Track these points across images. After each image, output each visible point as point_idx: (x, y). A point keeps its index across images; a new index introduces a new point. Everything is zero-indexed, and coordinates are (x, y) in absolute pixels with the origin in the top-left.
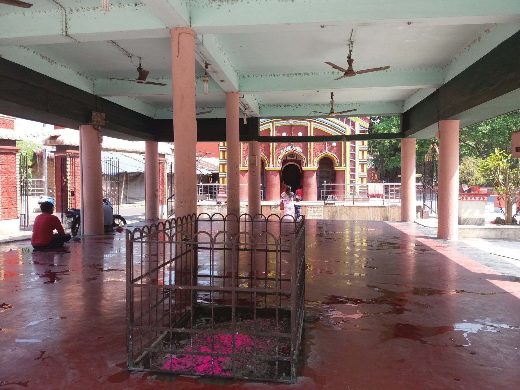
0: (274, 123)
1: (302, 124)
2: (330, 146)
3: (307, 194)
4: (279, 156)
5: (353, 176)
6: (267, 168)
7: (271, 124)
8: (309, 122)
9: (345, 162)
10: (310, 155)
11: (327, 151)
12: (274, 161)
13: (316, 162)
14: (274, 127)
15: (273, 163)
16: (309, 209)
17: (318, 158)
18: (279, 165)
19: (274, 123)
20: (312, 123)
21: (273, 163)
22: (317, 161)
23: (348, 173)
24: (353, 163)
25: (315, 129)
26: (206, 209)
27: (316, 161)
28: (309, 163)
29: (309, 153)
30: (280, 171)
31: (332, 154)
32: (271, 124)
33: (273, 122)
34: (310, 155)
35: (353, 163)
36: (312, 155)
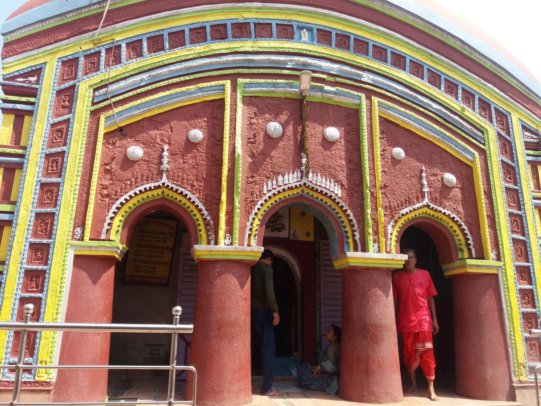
1: (337, 99)
3: (368, 372)
4: (254, 203)
6: (202, 249)
7: (228, 83)
8: (363, 96)
9: (497, 245)
10: (375, 209)
11: (426, 201)
12: (237, 220)
13: (394, 238)
14: (239, 96)
17: (399, 224)
18: (253, 242)
19: (240, 80)
20: (376, 100)
21: (230, 231)
22: (395, 233)
25: (384, 121)
27: (393, 233)
28: (371, 238)
29: (368, 201)
30: (255, 270)
31: (450, 213)
33: (233, 78)
34: (375, 209)
36: (381, 211)
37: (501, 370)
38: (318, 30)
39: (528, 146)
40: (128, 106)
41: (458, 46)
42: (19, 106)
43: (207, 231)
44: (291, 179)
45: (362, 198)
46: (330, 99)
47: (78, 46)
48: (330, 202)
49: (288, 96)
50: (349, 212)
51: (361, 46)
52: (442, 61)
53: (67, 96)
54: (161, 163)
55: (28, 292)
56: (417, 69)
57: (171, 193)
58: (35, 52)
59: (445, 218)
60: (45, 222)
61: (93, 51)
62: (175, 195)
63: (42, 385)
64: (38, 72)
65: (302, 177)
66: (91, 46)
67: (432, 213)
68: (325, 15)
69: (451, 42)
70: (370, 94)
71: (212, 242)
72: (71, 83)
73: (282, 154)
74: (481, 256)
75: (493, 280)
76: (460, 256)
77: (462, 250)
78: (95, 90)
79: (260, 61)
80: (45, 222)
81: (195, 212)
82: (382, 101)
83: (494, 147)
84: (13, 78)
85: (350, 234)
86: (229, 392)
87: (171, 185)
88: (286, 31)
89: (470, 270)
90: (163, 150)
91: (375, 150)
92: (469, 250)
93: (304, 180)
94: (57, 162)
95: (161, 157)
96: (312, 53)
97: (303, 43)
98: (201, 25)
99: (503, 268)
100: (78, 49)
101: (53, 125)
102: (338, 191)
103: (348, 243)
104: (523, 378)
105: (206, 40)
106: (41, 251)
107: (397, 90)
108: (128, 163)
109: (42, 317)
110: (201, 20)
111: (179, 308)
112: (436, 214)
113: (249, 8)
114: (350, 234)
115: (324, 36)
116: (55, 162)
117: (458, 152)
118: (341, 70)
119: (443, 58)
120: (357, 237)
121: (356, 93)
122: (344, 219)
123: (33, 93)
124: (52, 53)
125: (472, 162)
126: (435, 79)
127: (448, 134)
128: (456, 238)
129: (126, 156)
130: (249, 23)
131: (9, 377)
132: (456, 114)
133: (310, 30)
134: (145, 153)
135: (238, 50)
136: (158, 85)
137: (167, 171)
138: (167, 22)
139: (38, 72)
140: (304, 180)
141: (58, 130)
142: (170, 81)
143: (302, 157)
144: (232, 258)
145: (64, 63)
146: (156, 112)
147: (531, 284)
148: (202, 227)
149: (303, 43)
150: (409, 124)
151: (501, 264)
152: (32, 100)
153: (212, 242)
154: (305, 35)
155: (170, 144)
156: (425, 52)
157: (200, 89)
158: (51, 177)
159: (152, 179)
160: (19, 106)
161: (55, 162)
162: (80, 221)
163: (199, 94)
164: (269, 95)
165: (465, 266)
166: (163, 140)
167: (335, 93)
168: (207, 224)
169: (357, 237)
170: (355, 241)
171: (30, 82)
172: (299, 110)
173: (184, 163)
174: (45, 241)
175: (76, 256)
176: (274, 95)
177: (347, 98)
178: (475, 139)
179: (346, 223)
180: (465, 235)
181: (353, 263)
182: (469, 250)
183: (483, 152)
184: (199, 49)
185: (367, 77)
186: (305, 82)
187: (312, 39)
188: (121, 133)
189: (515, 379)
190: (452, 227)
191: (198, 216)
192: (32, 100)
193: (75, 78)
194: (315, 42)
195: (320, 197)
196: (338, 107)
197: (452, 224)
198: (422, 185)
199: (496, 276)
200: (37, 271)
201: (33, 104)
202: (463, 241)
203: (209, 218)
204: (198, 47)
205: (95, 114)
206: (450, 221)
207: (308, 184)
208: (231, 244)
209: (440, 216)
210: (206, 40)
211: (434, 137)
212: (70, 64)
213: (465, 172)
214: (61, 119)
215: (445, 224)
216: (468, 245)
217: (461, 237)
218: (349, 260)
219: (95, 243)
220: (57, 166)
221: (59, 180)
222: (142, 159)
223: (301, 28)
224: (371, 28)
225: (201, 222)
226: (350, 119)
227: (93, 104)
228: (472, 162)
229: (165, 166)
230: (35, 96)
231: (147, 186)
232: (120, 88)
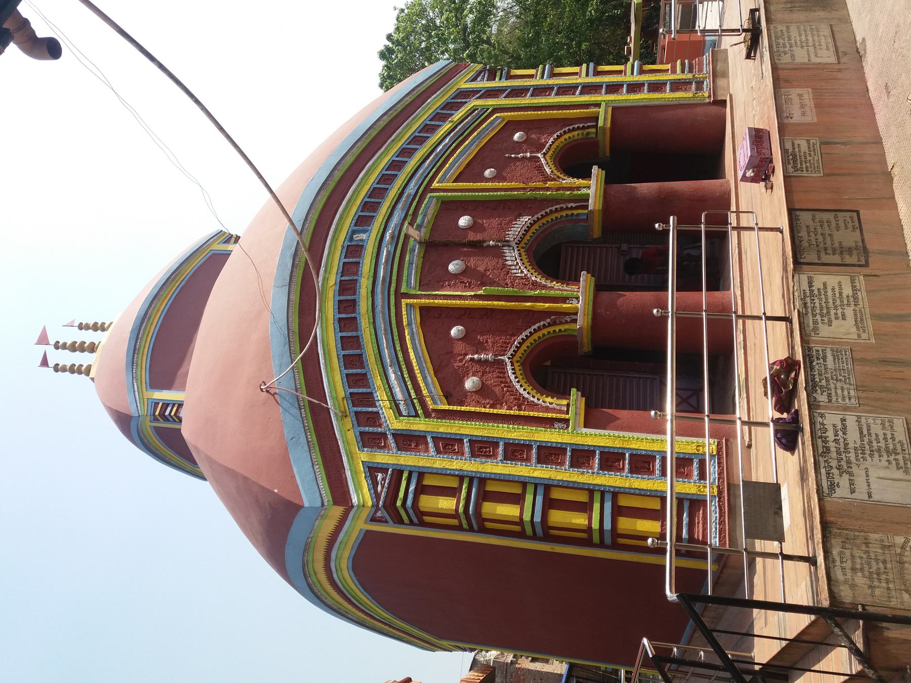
0: (403, 289)
2: (525, 147)
5: (634, 87)
7: (404, 302)
8: (429, 195)
11: (539, 155)
15: (564, 300)
16: (785, 59)
19: (403, 289)
20: (435, 185)
21: (564, 300)
23: (623, 98)
24: (589, 89)
26: (844, 481)
32: (404, 302)
33: (400, 296)
35: (589, 89)
37: (699, 110)
38: (355, 225)
39: (492, 77)
40: (422, 385)
41: (387, 119)
42: (412, 488)
43: (561, 323)
44: (512, 256)
45: (534, 200)
46: (429, 222)
47: (345, 433)
48: (536, 227)
49: (422, 255)
50: (548, 210)
51: (378, 193)
52: (400, 133)
54: (486, 361)
55: (623, 469)
56: (406, 152)
57: (519, 354)
58: (348, 474)
59: (557, 143)
60: (549, 454)
61: (354, 419)
62: (521, 351)
63: (721, 448)
64: (372, 470)
65: (509, 246)
67: (551, 152)
68: (341, 218)
69: (382, 124)
70: (428, 189)
71: (574, 317)
72: (390, 437)
73: (482, 264)
74: (596, 119)
75: (617, 111)
76: (594, 136)
77: (588, 134)
78: (401, 415)
79: (385, 273)
80: (549, 454)
81: (540, 334)
82: (437, 179)
85: (570, 212)
86: (723, 299)
87: (511, 352)
88: (354, 250)
89: (609, 125)
90: (472, 360)
91: (489, 184)
92: (589, 127)
93: (513, 244)
94: (481, 448)
95: (479, 361)
96: (381, 230)
97: (370, 238)
98: (336, 322)
99: (607, 103)
101: (438, 452)
102: (526, 219)
103: (578, 215)
104: (706, 95)
105: (355, 318)
106: (581, 457)
107: (427, 168)
108: (483, 391)
109: (650, 453)
110: (331, 321)
111: (657, 225)
112: (553, 149)
113: (324, 279)
114: (570, 212)
115: (363, 221)
116: (482, 448)
117: (493, 129)
118: (402, 210)
119: (398, 132)
120: (574, 205)
121: (427, 200)
122: (553, 216)
123: (398, 473)
124: (352, 457)
125: (503, 119)
126: (418, 140)
127: (475, 134)
128: (576, 137)
129: (476, 392)
130: (341, 281)
131: (715, 479)
132: (456, 127)
133: (354, 232)
134: (474, 375)
135: (370, 289)
136: (401, 359)
137: (496, 356)
138: (329, 351)
139: (372, 470)
140: (513, 244)
141: (444, 448)
142: (398, 348)
143: (489, 246)
144: (591, 298)
145: (364, 446)
146: (430, 365)
147: (623, 85)
148: (557, 328)
149: (370, 238)
150: (461, 163)
151: (603, 104)
152: (405, 475)
153: (574, 317)
154: (357, 237)
155: (466, 354)
156: (389, 145)
157: (409, 324)
158: (497, 453)
159: (504, 373)
160: (412, 488)
161: (482, 448)
162: (548, 423)
163: (414, 326)
164: (419, 271)
165: (604, 128)
166: (461, 361)
167: (425, 216)
168: (554, 323)
169: (574, 205)
170: (577, 208)
171: (384, 479)
172: (439, 247)
173: (487, 342)
174: (569, 454)
175: (585, 427)
176: (420, 267)
177: (429, 208)
178: (482, 116)
179: (558, 215)
180: (574, 129)
181: (599, 206)
182: (589, 127)
183: (496, 110)
184: (365, 323)
185: (411, 189)
186: (413, 232)
187: (365, 232)
188: (453, 391)
189: (708, 100)
190: (565, 140)
191: (545, 331)
192: (405, 475)
193: (384, 435)
194: (369, 228)
195: (530, 234)
196: (437, 217)
197: (562, 139)
198: (523, 158)
199: (614, 109)
200: (600, 460)
201: (410, 473)
202: (580, 132)
203: (548, 320)
204: (363, 324)
205: (427, 414)
206: (559, 140)
207: (516, 241)
208: (577, 298)
209: (554, 146)
210: (355, 318)
211: (477, 146)
213: (512, 126)
214: (431, 445)
215: (561, 145)
216: (584, 128)
217: (576, 133)
218: (597, 208)
220: (486, 448)
221: (501, 444)
222: (481, 378)
223: (351, 239)
224: (360, 183)
225: (551, 329)
226: (451, 208)
227: (417, 415)
228: (503, 119)
229: (490, 357)
230: (401, 472)
231: (510, 372)
232: (401, 390)
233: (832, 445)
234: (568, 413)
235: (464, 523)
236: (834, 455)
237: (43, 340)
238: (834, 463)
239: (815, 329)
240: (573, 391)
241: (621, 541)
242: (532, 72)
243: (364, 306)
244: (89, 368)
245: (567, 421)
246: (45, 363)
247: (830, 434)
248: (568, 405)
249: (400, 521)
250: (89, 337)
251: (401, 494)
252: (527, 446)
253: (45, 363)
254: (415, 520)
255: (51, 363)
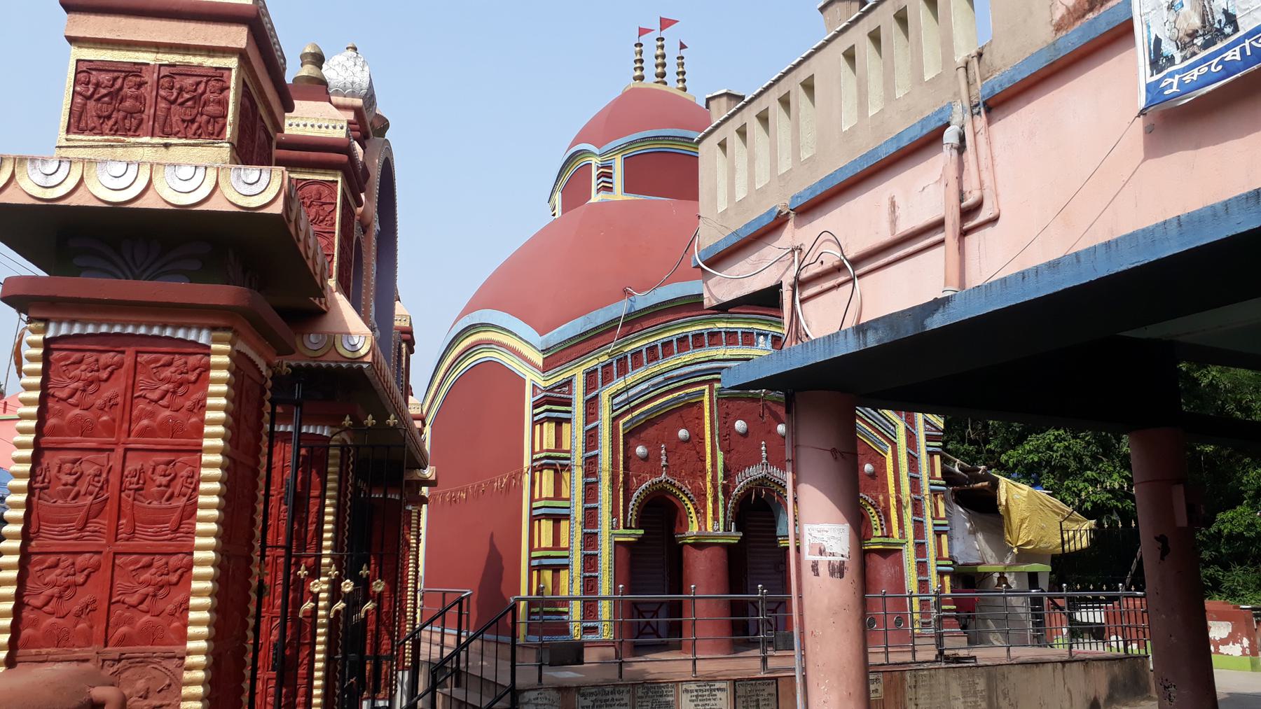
53: (591, 406)
64: (569, 383)
66: (606, 357)
83: (902, 440)
84: (551, 390)
88: (749, 338)
100: (596, 362)
133: (766, 336)
139: (569, 383)
162: (614, 513)
183: (894, 444)
212: (590, 375)
219: (628, 532)
223: (759, 334)
230: (570, 405)
233: (610, 697)
234: (625, 527)
235: (537, 456)
236: (604, 698)
237: (665, 23)
238: (600, 697)
239: (687, 691)
240: (642, 532)
241: (535, 573)
242: (938, 474)
243: (701, 354)
244: (641, 78)
245: (618, 528)
246: (643, 32)
247: (617, 696)
248: (631, 528)
249: (535, 407)
250: (671, 77)
251: (554, 408)
252: (595, 499)
253: (643, 32)
254: (536, 418)
255: (643, 40)
